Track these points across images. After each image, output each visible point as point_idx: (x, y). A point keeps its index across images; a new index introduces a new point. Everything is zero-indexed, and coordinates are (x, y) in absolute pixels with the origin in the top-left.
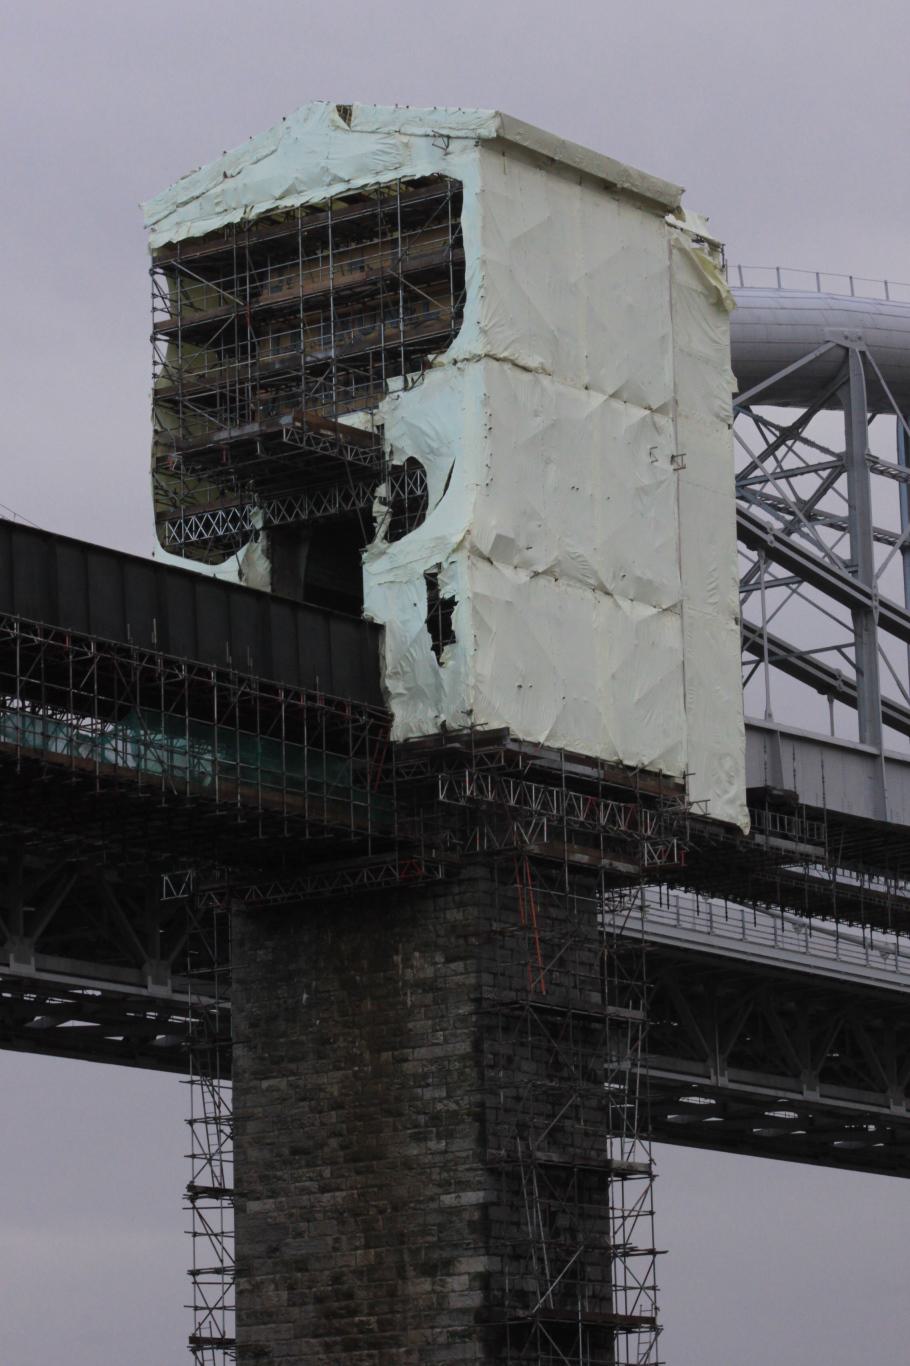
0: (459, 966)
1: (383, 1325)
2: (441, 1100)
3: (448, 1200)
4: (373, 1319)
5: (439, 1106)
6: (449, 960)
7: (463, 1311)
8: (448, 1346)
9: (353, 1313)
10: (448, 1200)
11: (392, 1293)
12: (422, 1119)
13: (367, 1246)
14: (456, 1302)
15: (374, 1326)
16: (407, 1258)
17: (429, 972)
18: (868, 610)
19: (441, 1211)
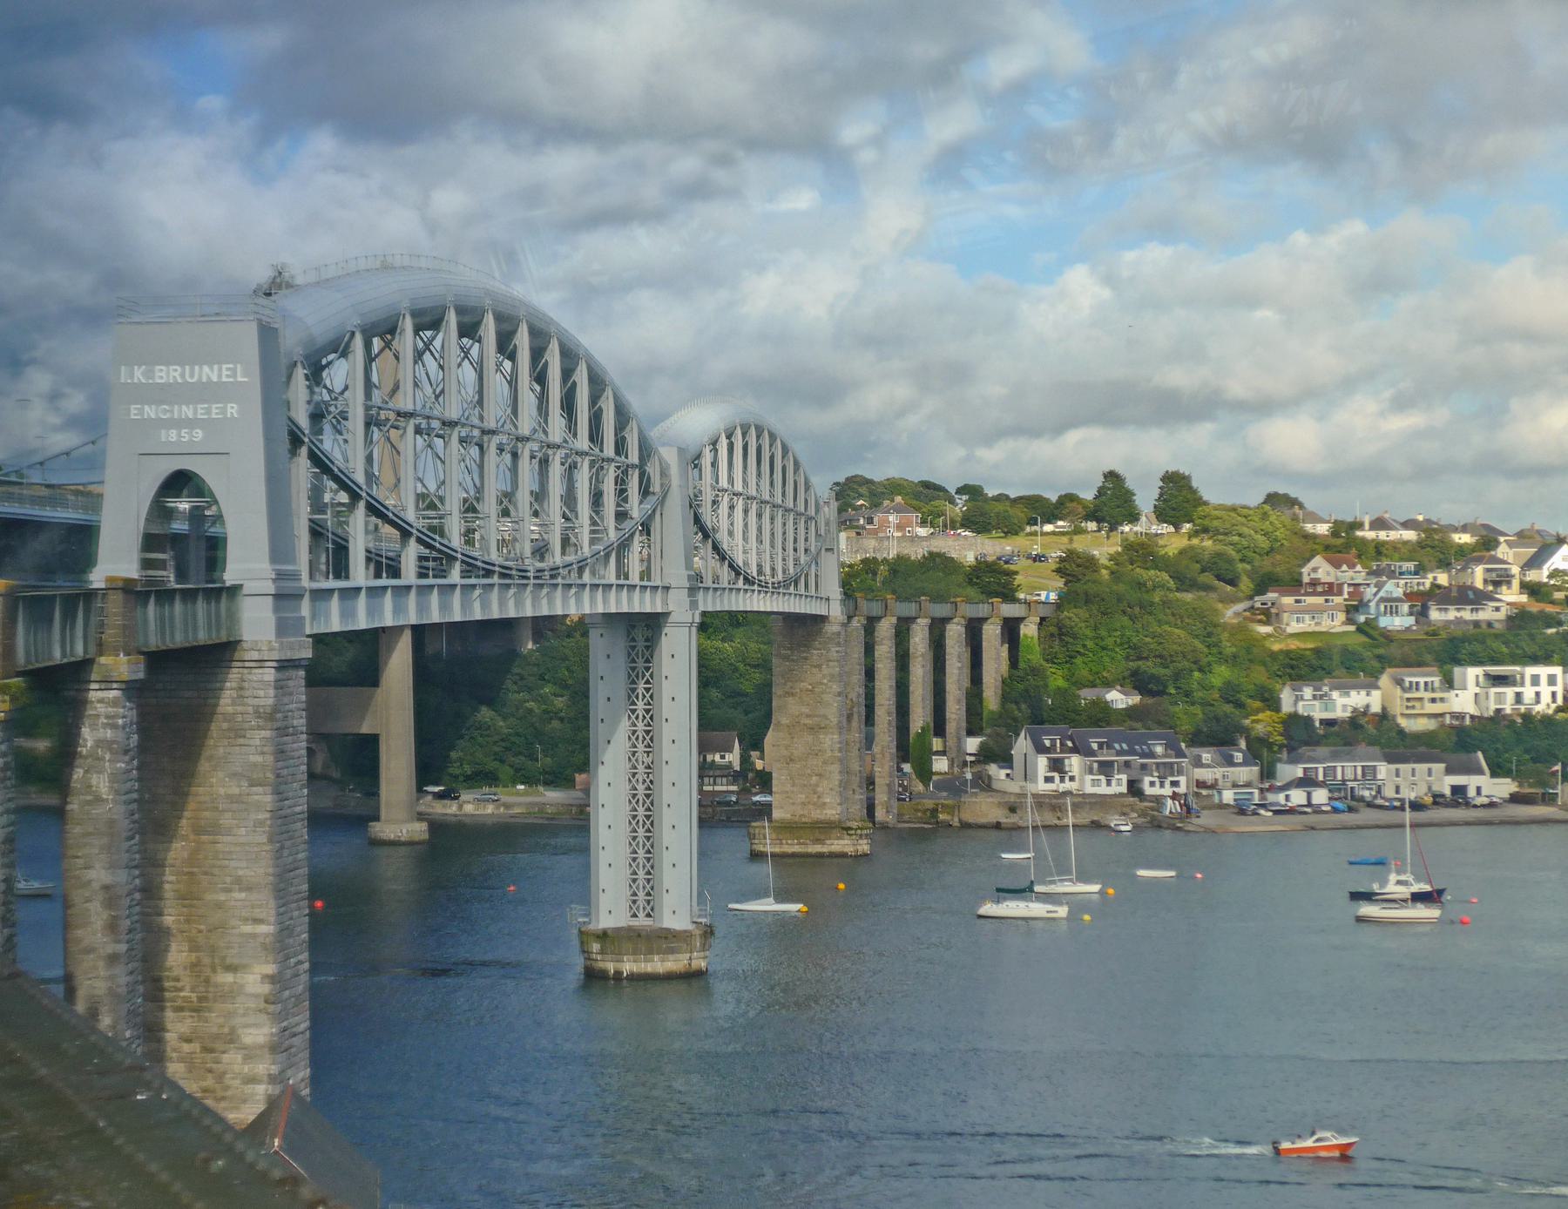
0: (260, 789)
1: (200, 999)
2: (242, 868)
3: (248, 929)
4: (194, 995)
5: (240, 873)
6: (251, 785)
7: (256, 996)
8: (244, 1015)
9: (181, 990)
10: (248, 929)
11: (207, 981)
12: (228, 879)
13: (190, 951)
14: (250, 989)
15: (195, 999)
16: (216, 961)
17: (236, 791)
18: (409, 534)
19: (242, 935)
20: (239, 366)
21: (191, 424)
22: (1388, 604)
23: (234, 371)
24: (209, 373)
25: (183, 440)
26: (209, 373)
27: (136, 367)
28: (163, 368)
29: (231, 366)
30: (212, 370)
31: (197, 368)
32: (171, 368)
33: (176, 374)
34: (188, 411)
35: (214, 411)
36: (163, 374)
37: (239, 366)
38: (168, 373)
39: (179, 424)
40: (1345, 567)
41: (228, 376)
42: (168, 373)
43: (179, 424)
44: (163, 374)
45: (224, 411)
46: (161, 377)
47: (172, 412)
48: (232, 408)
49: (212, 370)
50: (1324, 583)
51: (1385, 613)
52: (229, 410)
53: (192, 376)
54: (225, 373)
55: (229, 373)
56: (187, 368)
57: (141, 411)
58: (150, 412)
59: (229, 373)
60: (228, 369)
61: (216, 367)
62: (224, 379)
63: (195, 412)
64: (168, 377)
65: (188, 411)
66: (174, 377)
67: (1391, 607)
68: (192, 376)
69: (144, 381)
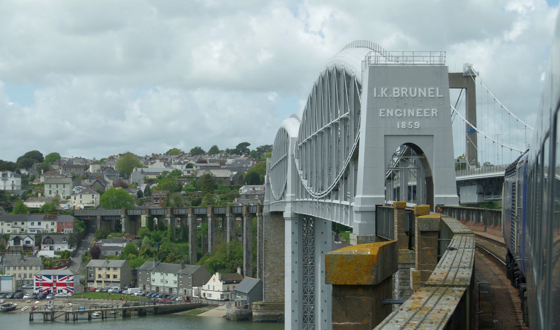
20: (437, 89)
21: (414, 118)
23: (434, 91)
24: (423, 92)
25: (409, 127)
26: (423, 92)
27: (382, 89)
28: (397, 88)
29: (433, 89)
30: (423, 90)
31: (415, 89)
32: (402, 89)
33: (405, 92)
34: (411, 112)
35: (425, 113)
36: (398, 92)
37: (437, 89)
38: (400, 92)
39: (407, 118)
42: (400, 92)
43: (407, 118)
44: (398, 92)
45: (429, 112)
46: (396, 94)
47: (402, 112)
48: (434, 111)
49: (423, 90)
52: (433, 113)
53: (413, 93)
54: (430, 92)
55: (432, 92)
57: (385, 112)
58: (390, 112)
60: (431, 90)
61: (425, 89)
62: (430, 96)
64: (400, 95)
65: (411, 112)
68: (413, 93)
69: (386, 96)
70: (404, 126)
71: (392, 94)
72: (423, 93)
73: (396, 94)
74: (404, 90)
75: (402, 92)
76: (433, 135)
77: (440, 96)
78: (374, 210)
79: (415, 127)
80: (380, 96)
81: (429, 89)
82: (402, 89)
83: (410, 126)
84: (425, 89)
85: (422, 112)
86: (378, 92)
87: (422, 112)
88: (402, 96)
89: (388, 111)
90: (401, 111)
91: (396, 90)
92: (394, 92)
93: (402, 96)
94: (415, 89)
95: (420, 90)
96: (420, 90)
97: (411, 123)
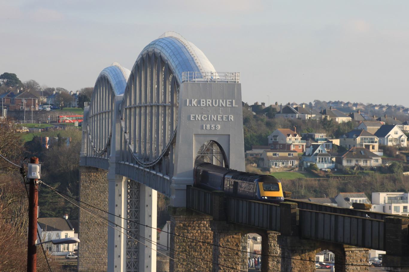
22: (321, 157)
23: (232, 102)
25: (212, 129)
27: (193, 100)
29: (231, 100)
31: (217, 101)
33: (210, 103)
37: (234, 101)
40: (291, 136)
41: (229, 104)
44: (204, 103)
50: (280, 144)
51: (319, 162)
52: (230, 118)
53: (216, 104)
54: (228, 103)
55: (230, 103)
56: (214, 101)
57: (195, 117)
59: (230, 103)
61: (224, 101)
63: (217, 117)
66: (209, 104)
67: (322, 159)
68: (216, 104)
69: (196, 105)
70: (208, 128)
71: (200, 105)
72: (223, 104)
73: (203, 104)
74: (209, 101)
75: (208, 103)
76: (229, 135)
77: (236, 106)
78: (185, 188)
79: (216, 129)
80: (191, 105)
81: (228, 101)
82: (208, 100)
83: (213, 128)
84: (224, 101)
85: (222, 118)
86: (191, 102)
87: (222, 118)
88: (207, 105)
89: (197, 116)
90: (206, 116)
91: (203, 101)
92: (202, 103)
93: (207, 105)
94: (217, 101)
95: (221, 101)
96: (221, 101)
97: (214, 125)
